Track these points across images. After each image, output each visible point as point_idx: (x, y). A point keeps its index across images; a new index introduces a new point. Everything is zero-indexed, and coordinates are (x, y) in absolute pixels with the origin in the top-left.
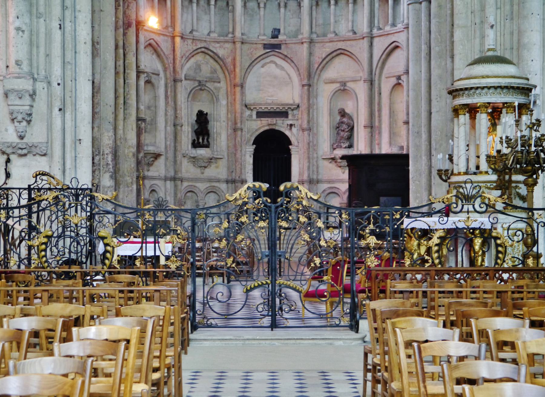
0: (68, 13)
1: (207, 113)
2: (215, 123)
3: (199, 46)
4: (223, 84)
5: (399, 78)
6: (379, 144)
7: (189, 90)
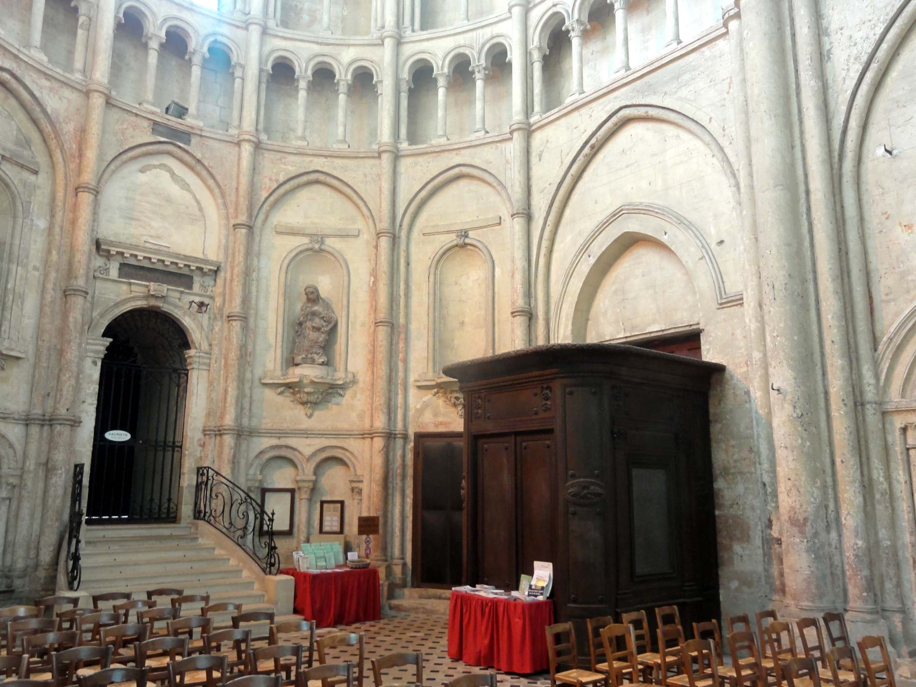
4: (42, 179)
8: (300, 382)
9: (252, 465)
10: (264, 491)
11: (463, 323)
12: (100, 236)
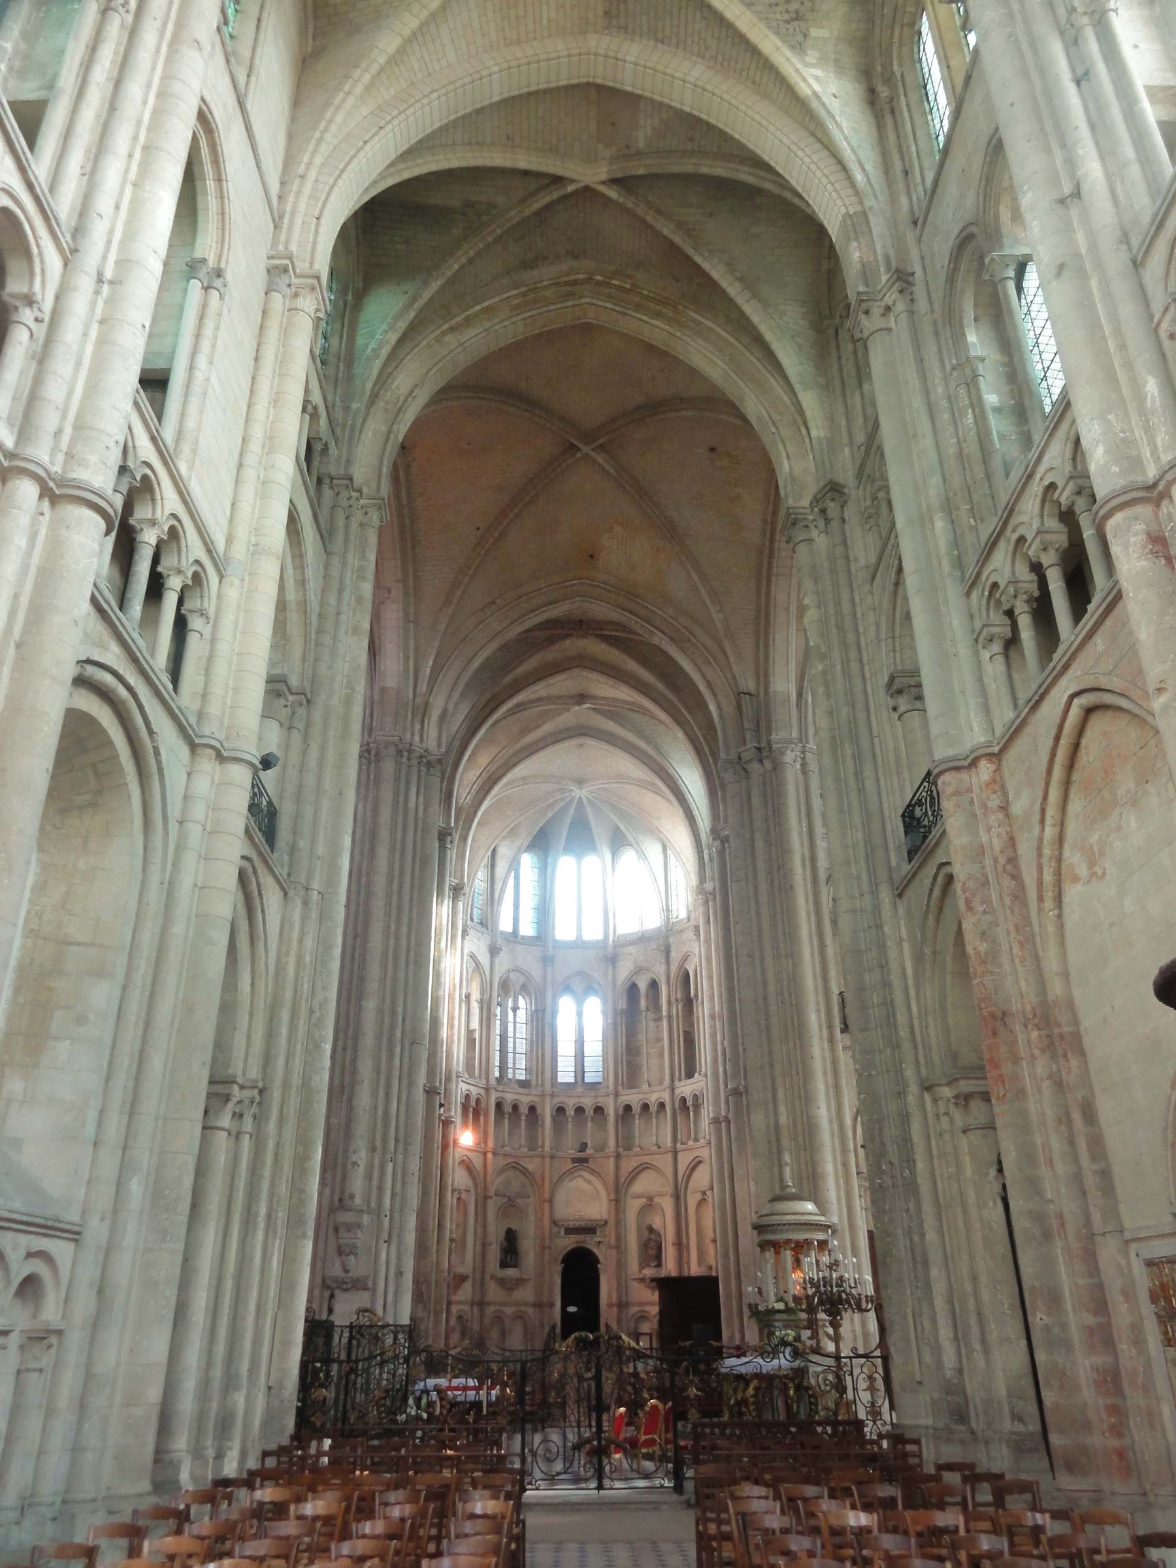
0: (401, 1145)
5: (704, 1193)
6: (689, 1263)
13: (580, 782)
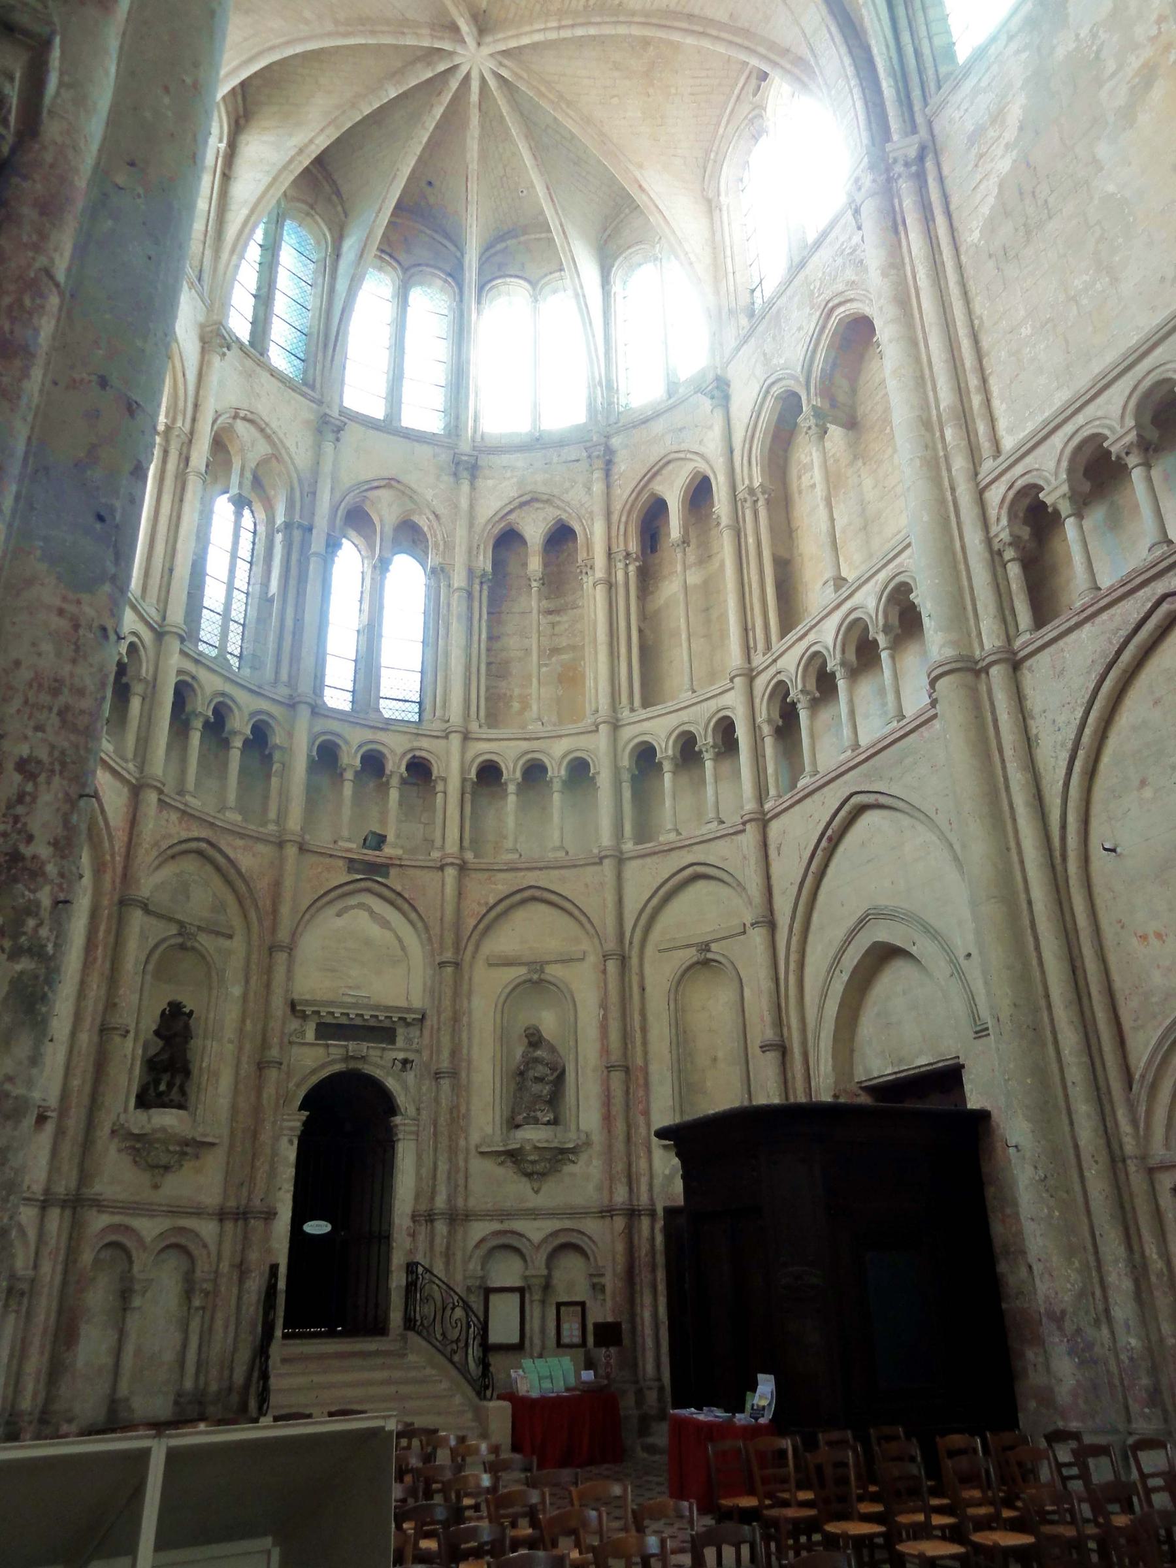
1: (192, 1012)
2: (208, 1043)
3: (196, 834)
4: (237, 945)
7: (151, 942)
8: (521, 1149)
9: (471, 1257)
10: (488, 1292)
11: (715, 1060)
12: (296, 997)
13: (483, 26)
